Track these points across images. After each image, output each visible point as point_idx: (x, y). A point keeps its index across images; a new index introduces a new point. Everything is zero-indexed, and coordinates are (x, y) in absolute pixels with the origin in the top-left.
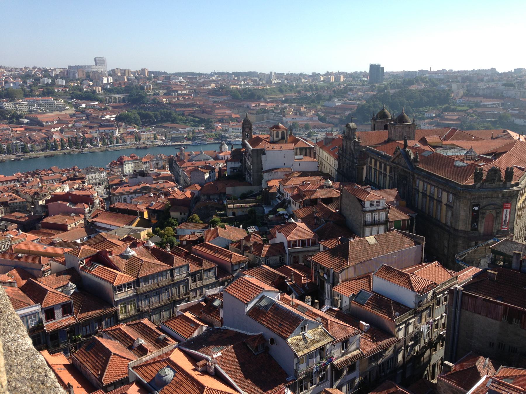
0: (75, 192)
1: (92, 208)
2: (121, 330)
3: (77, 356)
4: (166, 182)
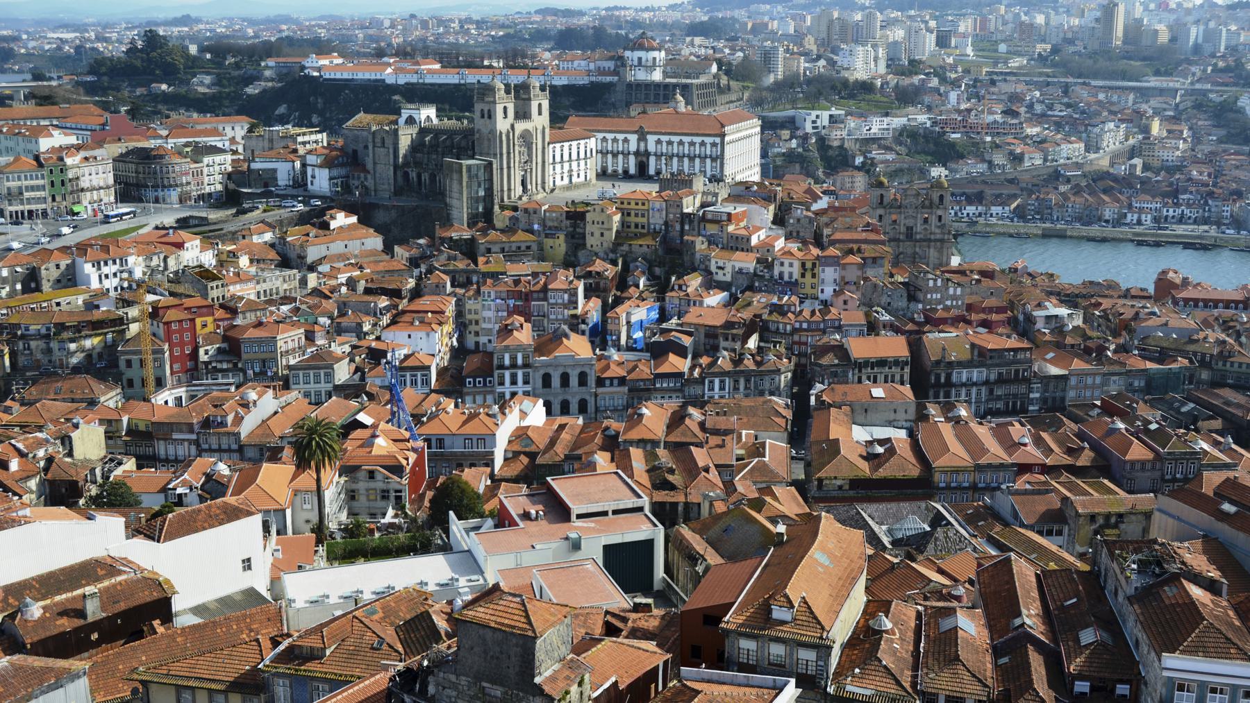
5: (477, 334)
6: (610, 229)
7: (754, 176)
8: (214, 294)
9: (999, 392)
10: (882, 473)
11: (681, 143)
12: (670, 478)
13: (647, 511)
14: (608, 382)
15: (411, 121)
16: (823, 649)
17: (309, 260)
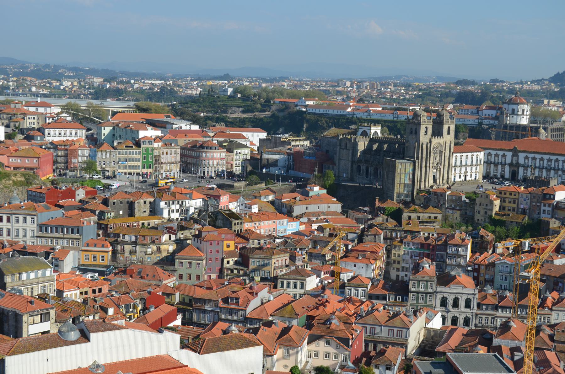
5: (398, 270)
6: (492, 210)
8: (236, 228)
11: (542, 159)
14: (484, 307)
15: (365, 134)
17: (295, 214)
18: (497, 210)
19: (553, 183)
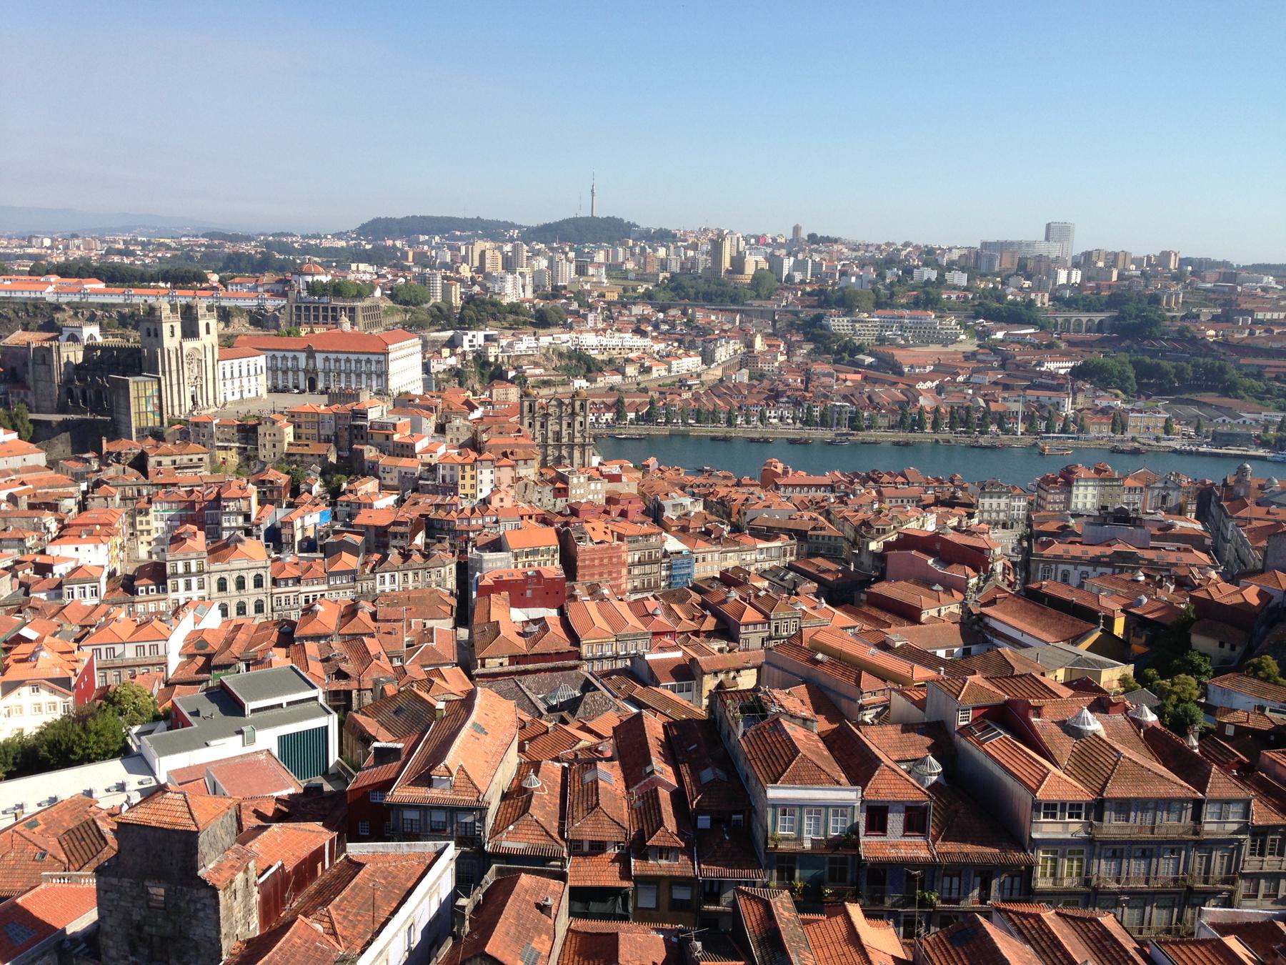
0: (952, 536)
1: (986, 580)
2: (1044, 922)
3: (928, 949)
4: (1186, 550)
6: (281, 441)
7: (417, 389)
9: (636, 571)
10: (538, 649)
11: (348, 360)
12: (343, 666)
13: (321, 700)
15: (74, 338)
16: (483, 810)
18: (292, 440)
19: (365, 397)
